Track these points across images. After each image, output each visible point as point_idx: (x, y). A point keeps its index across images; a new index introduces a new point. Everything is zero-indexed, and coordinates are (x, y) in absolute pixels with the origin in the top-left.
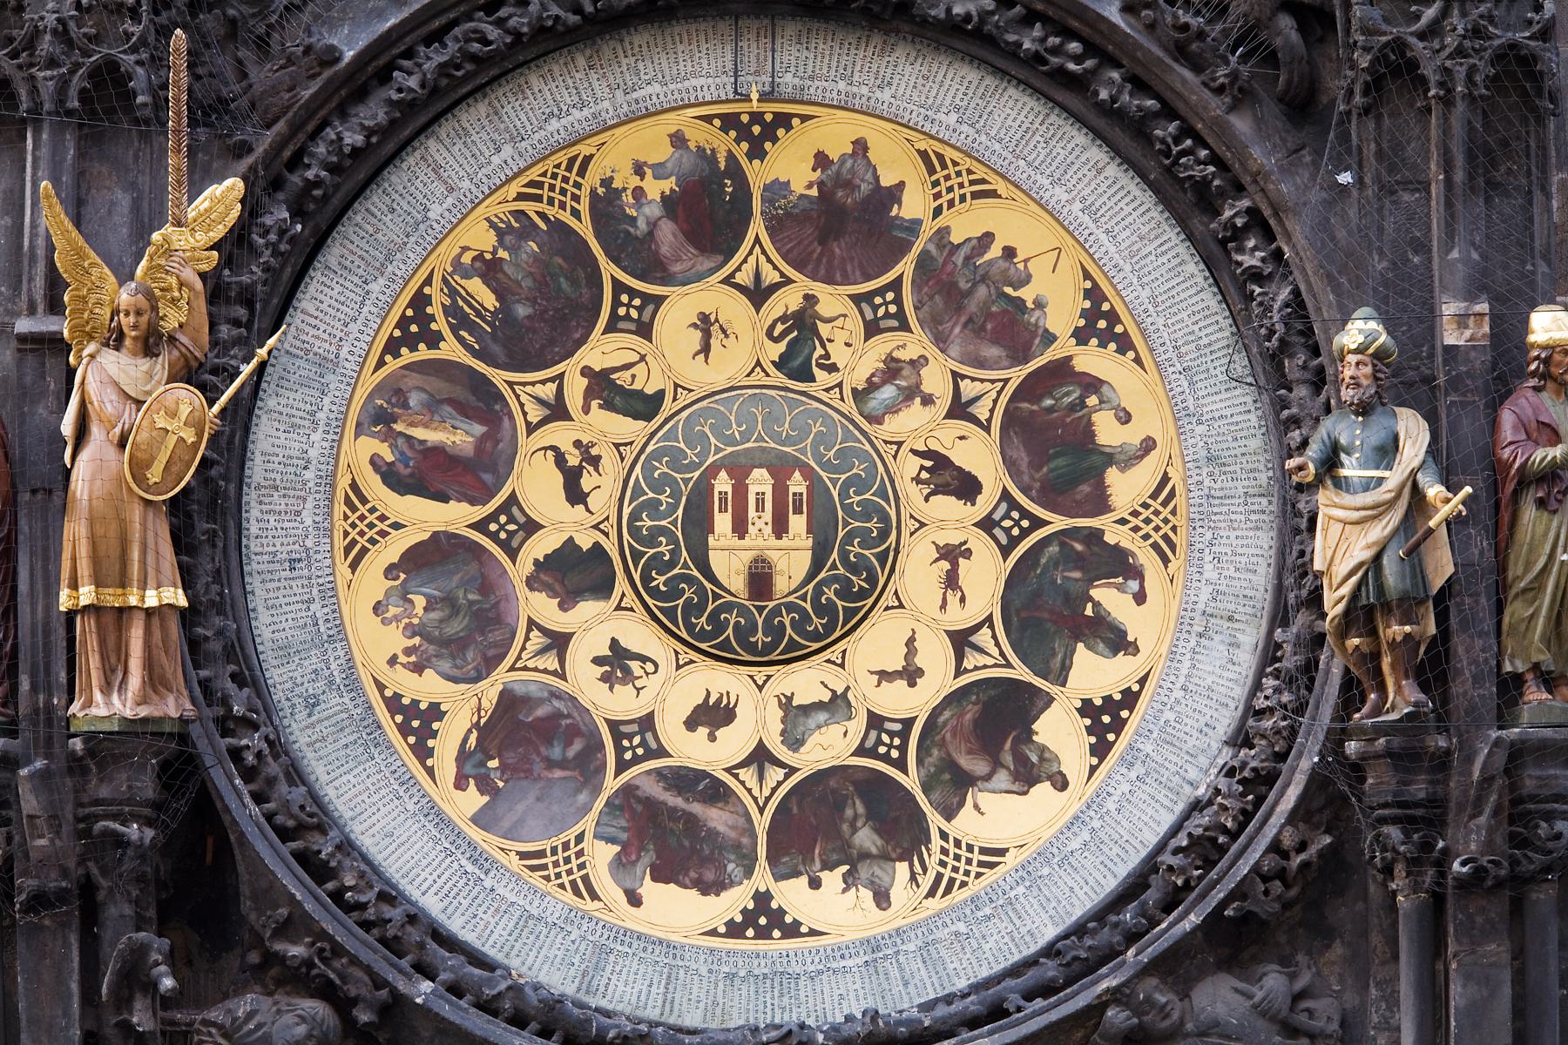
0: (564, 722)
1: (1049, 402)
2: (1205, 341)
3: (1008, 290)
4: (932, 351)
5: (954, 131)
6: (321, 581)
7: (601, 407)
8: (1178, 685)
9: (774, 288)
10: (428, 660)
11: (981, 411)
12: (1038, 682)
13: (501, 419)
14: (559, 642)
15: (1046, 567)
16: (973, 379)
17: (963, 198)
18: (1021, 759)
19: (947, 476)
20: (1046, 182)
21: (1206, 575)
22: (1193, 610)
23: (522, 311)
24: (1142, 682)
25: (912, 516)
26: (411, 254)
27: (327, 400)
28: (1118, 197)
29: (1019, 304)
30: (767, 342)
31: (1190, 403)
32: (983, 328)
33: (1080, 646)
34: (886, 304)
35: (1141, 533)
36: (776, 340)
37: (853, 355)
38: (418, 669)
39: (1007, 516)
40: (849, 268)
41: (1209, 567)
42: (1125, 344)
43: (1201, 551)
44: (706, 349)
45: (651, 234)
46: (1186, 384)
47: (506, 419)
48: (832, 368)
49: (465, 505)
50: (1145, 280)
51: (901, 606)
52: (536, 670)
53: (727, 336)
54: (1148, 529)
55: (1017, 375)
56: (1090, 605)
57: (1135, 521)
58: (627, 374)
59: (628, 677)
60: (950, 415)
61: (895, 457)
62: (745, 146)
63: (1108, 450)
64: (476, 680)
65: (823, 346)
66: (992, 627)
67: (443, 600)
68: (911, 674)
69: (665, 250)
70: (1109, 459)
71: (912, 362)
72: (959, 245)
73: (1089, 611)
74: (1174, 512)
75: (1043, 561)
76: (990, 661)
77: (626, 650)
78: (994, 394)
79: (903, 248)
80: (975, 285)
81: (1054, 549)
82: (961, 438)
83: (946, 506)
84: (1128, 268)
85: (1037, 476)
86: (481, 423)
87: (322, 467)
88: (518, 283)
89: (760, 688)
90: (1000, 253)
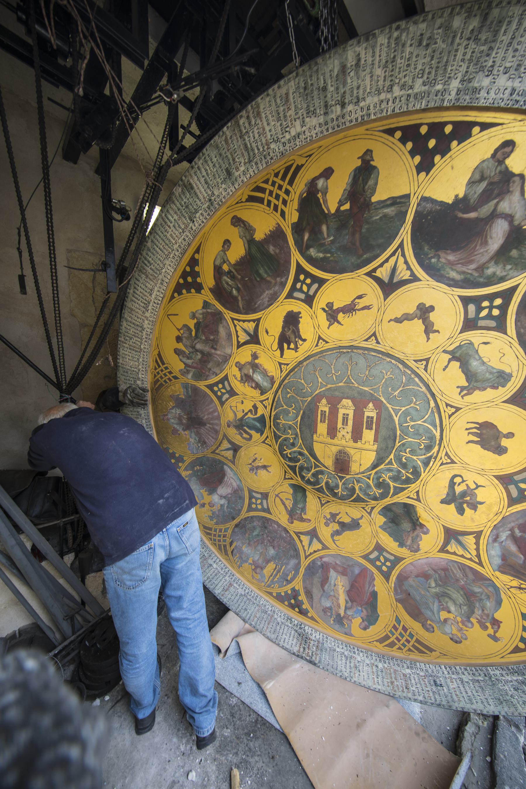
0: (518, 533)
1: (235, 292)
2: (176, 217)
3: (193, 334)
4: (232, 361)
5: (143, 380)
6: (446, 673)
7: (305, 514)
8: (389, 96)
9: (230, 442)
10: (488, 616)
11: (251, 327)
12: (410, 217)
13: (325, 562)
14: (451, 535)
15: (325, 252)
16: (238, 337)
17: (166, 368)
18: (486, 196)
19: (289, 333)
20: (144, 333)
21: (299, 129)
22: (326, 123)
23: (272, 552)
24: (390, 132)
25: (317, 345)
26: (261, 602)
27: (338, 649)
28: (137, 296)
29: (197, 326)
30: (252, 441)
31: (205, 206)
32: (213, 340)
33: (374, 199)
34: (219, 390)
35: (286, 197)
36: (251, 436)
37: (247, 400)
38: (496, 623)
39: (301, 290)
40: (211, 410)
41: (293, 133)
42: (193, 262)
43: (284, 144)
44: (265, 467)
45: (225, 497)
46: (198, 215)
47: (324, 560)
48: (255, 407)
49: (375, 583)
50: (162, 266)
51: (374, 334)
52: (478, 549)
53: (256, 459)
54: (282, 194)
55: (228, 315)
56: (342, 208)
57: (281, 206)
58: (287, 502)
59: (468, 492)
60: (258, 342)
61: (287, 365)
62: (180, 464)
63: (246, 245)
64: (497, 589)
65: (246, 414)
66: (374, 270)
67: (440, 602)
68: (424, 312)
69: (229, 491)
70: (251, 242)
71: (240, 370)
72: (185, 364)
73: (347, 206)
74: (266, 182)
75: (321, 255)
76: (401, 260)
77: (448, 494)
78: (241, 323)
79: (195, 390)
80: (197, 351)
81: (312, 252)
82: (267, 332)
83: (306, 327)
84: (160, 277)
85: (273, 281)
86: (329, 572)
87: (374, 658)
88: (261, 553)
89: (458, 409)
90: (181, 344)
